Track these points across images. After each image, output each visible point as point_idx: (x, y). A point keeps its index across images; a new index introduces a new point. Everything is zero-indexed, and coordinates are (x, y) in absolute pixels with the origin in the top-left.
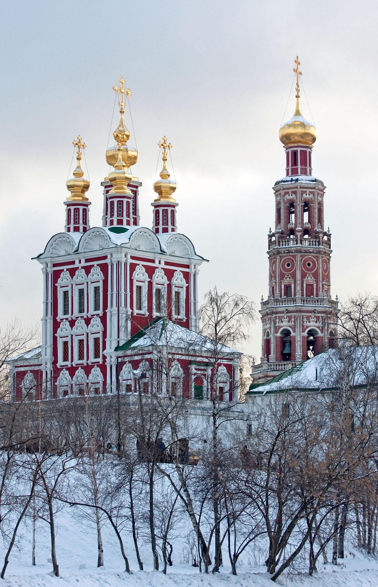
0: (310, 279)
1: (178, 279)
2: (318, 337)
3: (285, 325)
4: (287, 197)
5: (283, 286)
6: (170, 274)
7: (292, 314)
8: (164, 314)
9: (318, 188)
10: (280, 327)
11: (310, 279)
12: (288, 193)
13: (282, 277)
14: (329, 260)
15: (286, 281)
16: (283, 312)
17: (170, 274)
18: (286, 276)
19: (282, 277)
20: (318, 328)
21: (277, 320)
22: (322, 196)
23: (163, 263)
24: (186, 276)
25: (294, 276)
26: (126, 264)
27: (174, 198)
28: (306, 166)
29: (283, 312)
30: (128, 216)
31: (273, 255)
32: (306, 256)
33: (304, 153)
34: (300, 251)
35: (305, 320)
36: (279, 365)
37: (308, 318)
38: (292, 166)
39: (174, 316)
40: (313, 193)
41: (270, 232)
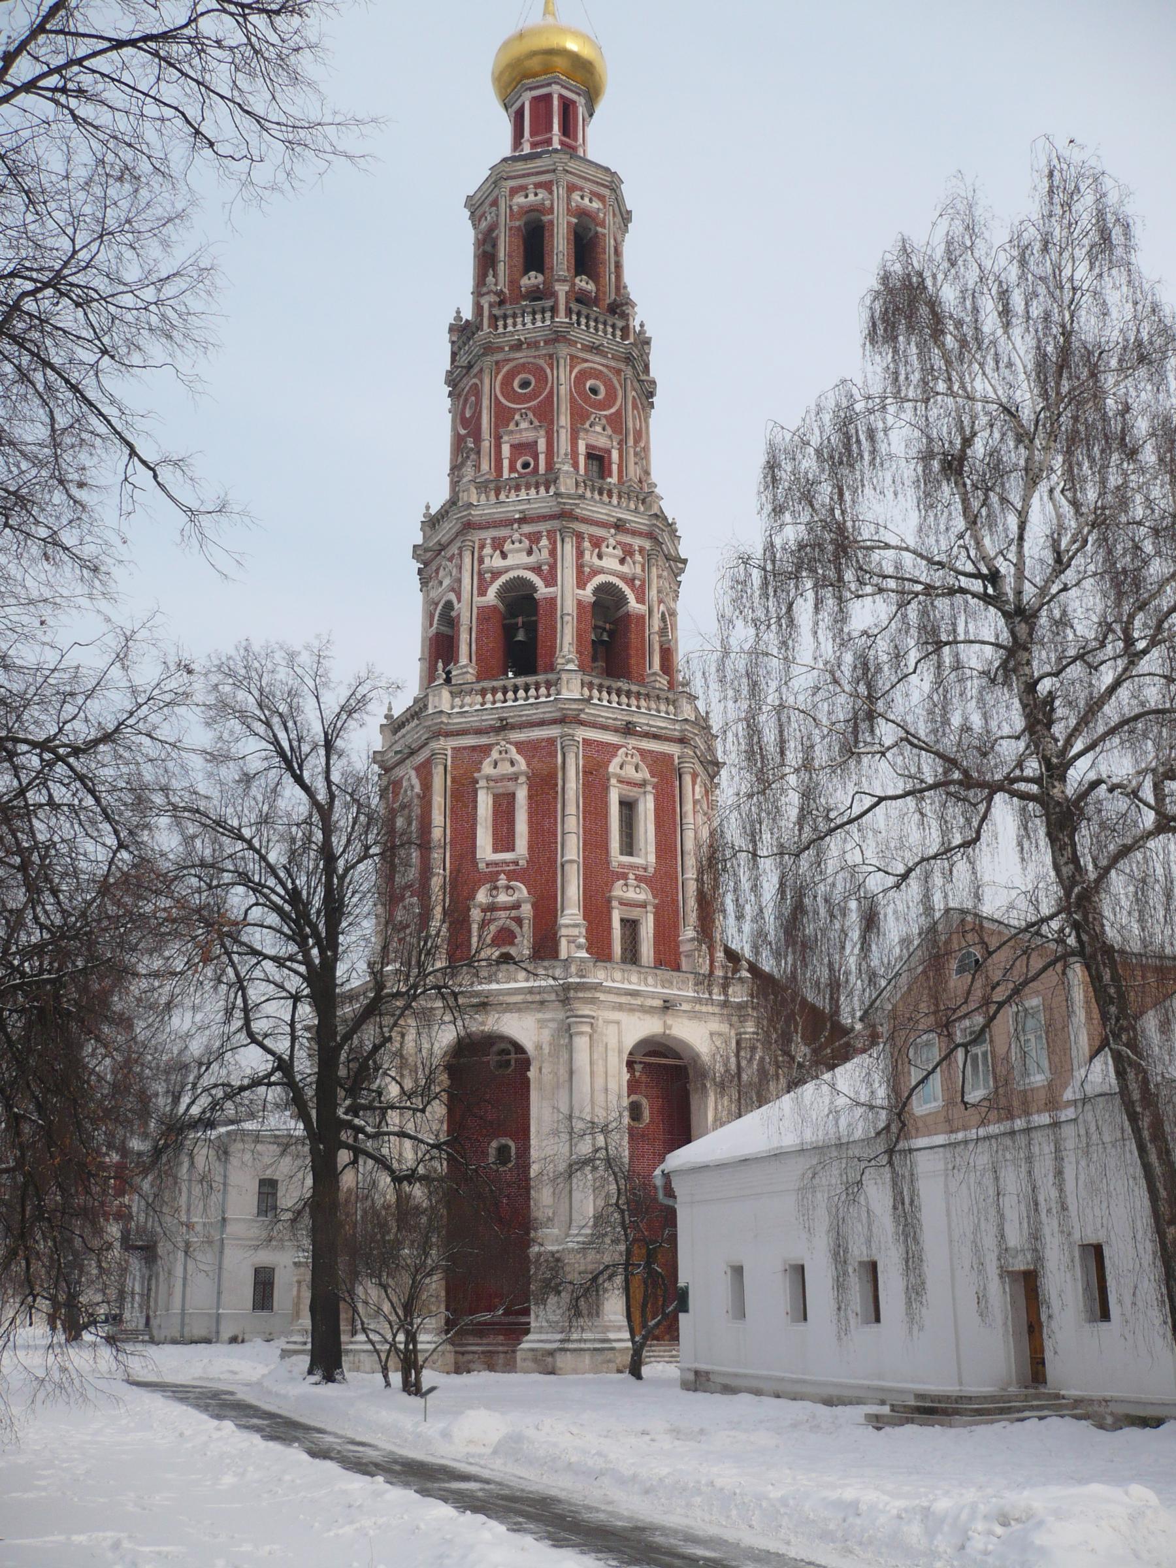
2: (628, 615)
3: (517, 562)
4: (519, 200)
5: (506, 450)
7: (542, 527)
10: (496, 574)
11: (599, 437)
12: (523, 188)
13: (503, 417)
16: (508, 523)
18: (517, 417)
19: (503, 417)
20: (630, 581)
21: (488, 550)
25: (545, 415)
28: (576, 140)
29: (508, 523)
32: (586, 361)
33: (567, 107)
35: (587, 544)
36: (494, 691)
37: (597, 543)
38: (532, 134)
40: (601, 198)
41: (458, 317)
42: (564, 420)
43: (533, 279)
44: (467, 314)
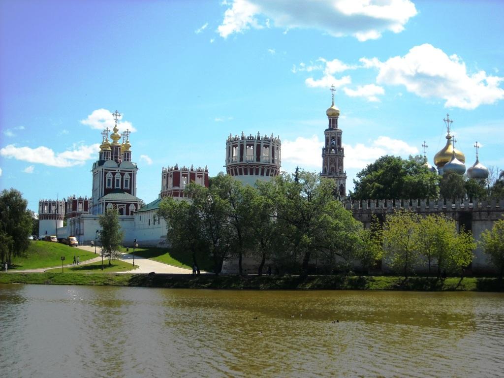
0: (333, 166)
1: (127, 176)
6: (122, 175)
8: (120, 187)
9: (340, 133)
11: (333, 166)
14: (343, 158)
15: (325, 166)
17: (122, 175)
22: (341, 135)
23: (120, 171)
24: (130, 175)
25: (327, 164)
26: (102, 172)
27: (130, 149)
30: (107, 156)
31: (324, 155)
34: (329, 156)
39: (124, 188)
40: (335, 134)
42: (328, 165)
43: (328, 146)
44: (324, 147)
